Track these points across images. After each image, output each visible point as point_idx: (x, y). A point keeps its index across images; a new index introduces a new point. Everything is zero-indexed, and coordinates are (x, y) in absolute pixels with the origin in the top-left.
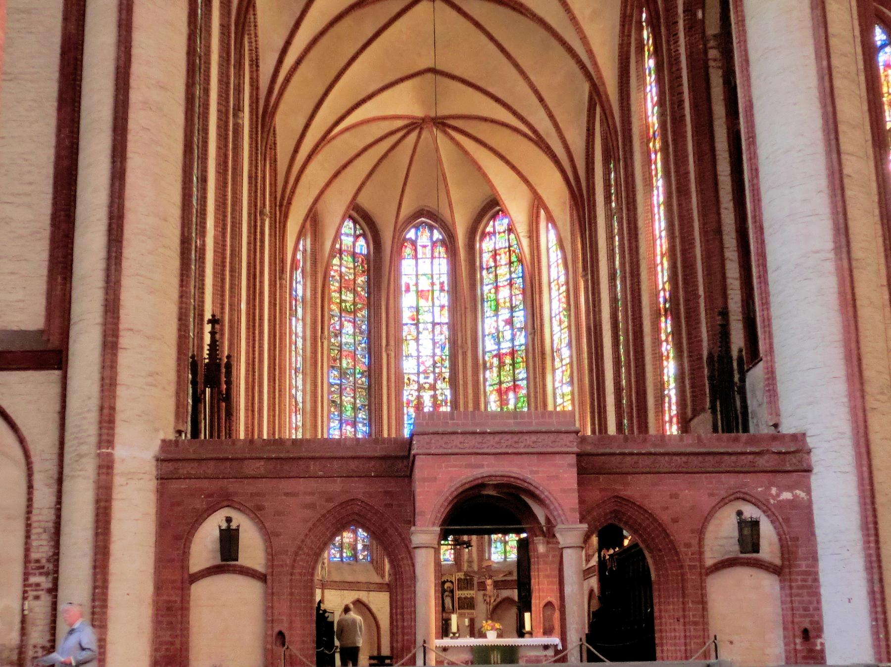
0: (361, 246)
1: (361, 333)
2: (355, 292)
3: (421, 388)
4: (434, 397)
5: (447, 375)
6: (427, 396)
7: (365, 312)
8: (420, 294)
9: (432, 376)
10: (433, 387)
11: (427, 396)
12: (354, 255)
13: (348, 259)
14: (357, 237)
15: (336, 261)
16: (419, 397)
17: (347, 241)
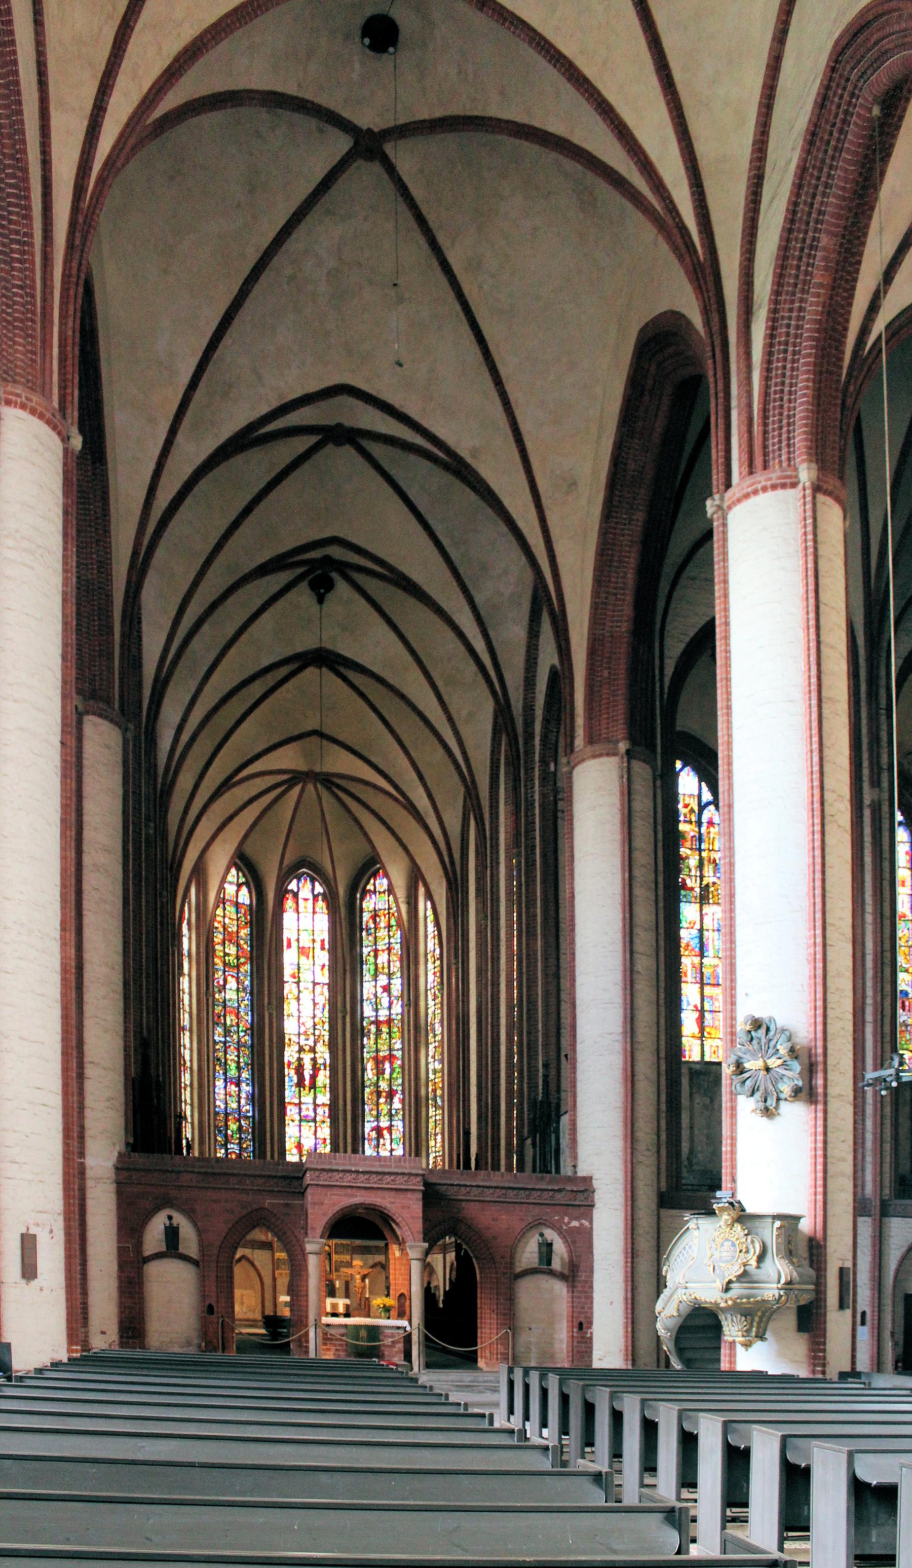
0: (244, 896)
1: (244, 989)
2: (238, 945)
3: (301, 1050)
4: (314, 1060)
5: (327, 1038)
6: (307, 1058)
7: (248, 967)
8: (302, 951)
9: (312, 1038)
10: (313, 1050)
11: (307, 1058)
12: (237, 905)
13: (231, 910)
14: (239, 886)
15: (219, 912)
16: (300, 1059)
17: (230, 890)
